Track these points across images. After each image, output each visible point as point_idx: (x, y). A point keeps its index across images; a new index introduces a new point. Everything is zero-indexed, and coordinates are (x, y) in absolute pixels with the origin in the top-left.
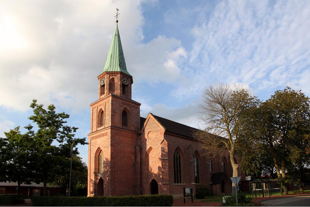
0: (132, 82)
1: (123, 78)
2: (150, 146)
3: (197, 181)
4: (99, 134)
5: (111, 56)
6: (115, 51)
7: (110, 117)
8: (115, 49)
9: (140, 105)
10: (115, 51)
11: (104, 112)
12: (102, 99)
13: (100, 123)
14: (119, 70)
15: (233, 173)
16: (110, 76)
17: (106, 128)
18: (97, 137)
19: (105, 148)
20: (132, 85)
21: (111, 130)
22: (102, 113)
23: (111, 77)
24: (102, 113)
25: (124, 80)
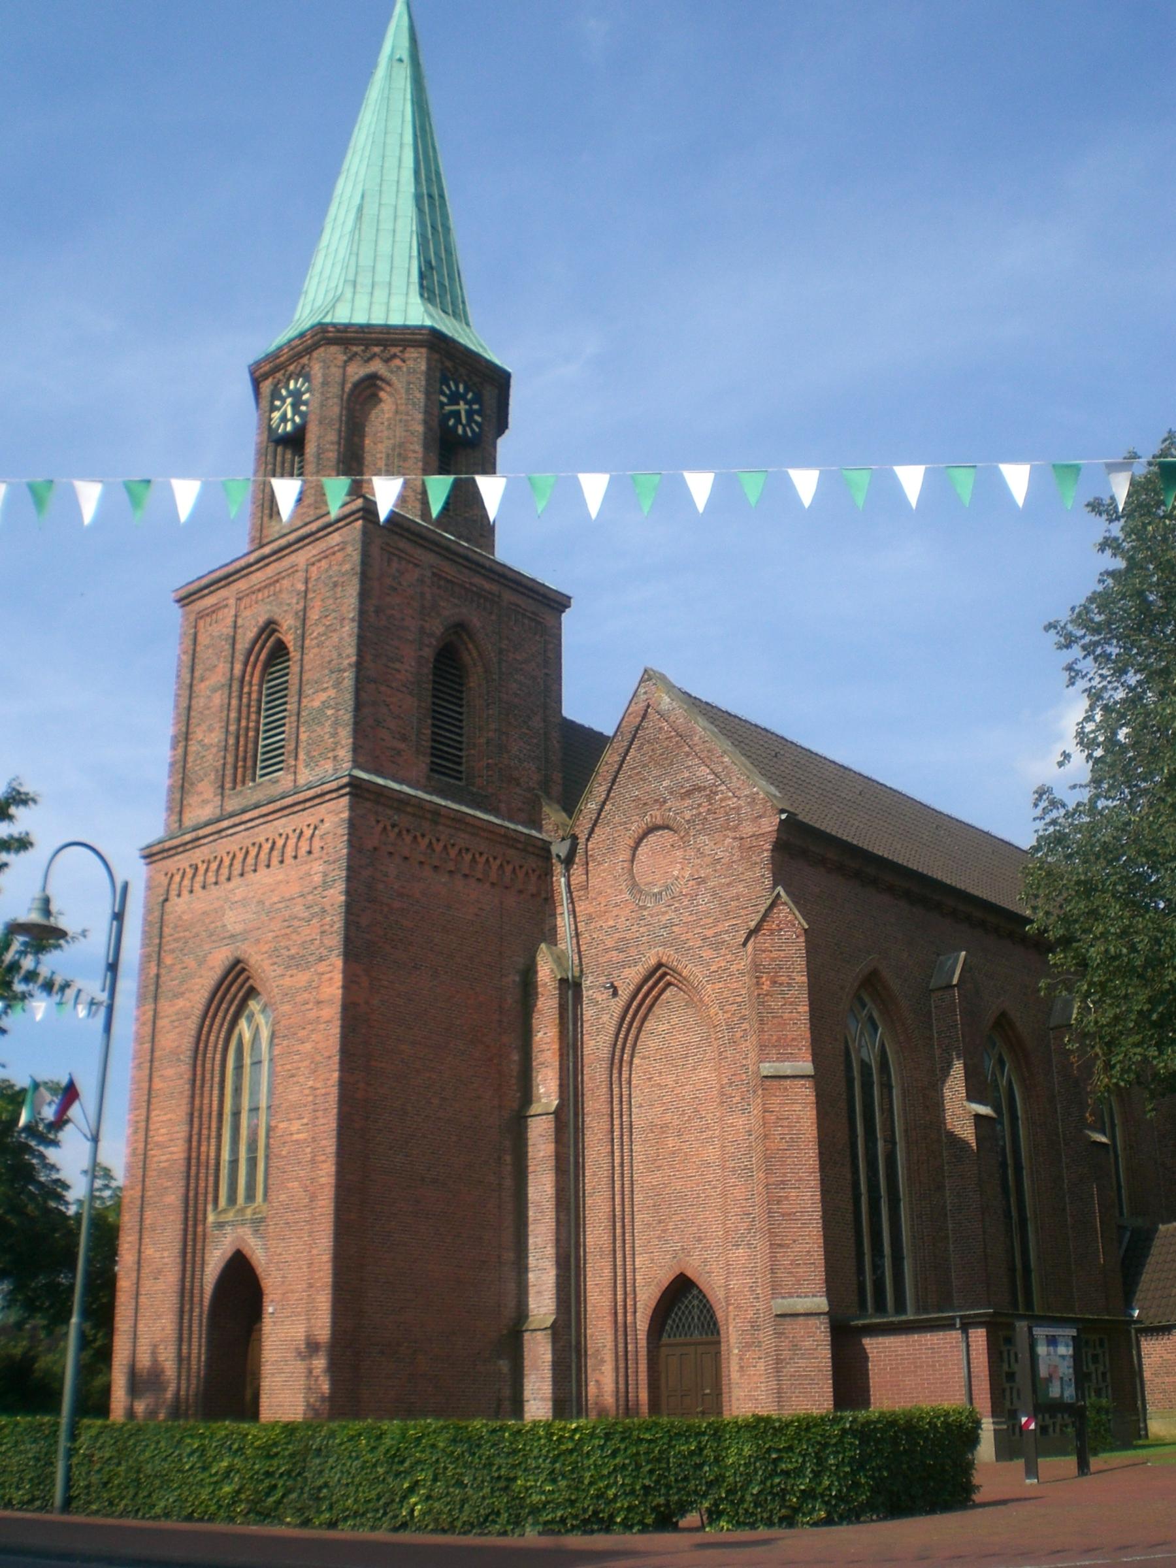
0: (502, 425)
1: (445, 381)
2: (653, 962)
3: (1020, 1299)
4: (186, 865)
5: (360, 209)
6: (392, 176)
7: (348, 698)
8: (391, 162)
9: (557, 603)
10: (392, 176)
11: (295, 655)
12: (283, 542)
13: (252, 752)
14: (409, 310)
15: (549, 1357)
16: (350, 359)
17: (231, 816)
18: (225, 871)
19: (297, 962)
20: (501, 442)
21: (352, 808)
22: (272, 652)
23: (357, 371)
24: (272, 652)
25: (454, 398)
